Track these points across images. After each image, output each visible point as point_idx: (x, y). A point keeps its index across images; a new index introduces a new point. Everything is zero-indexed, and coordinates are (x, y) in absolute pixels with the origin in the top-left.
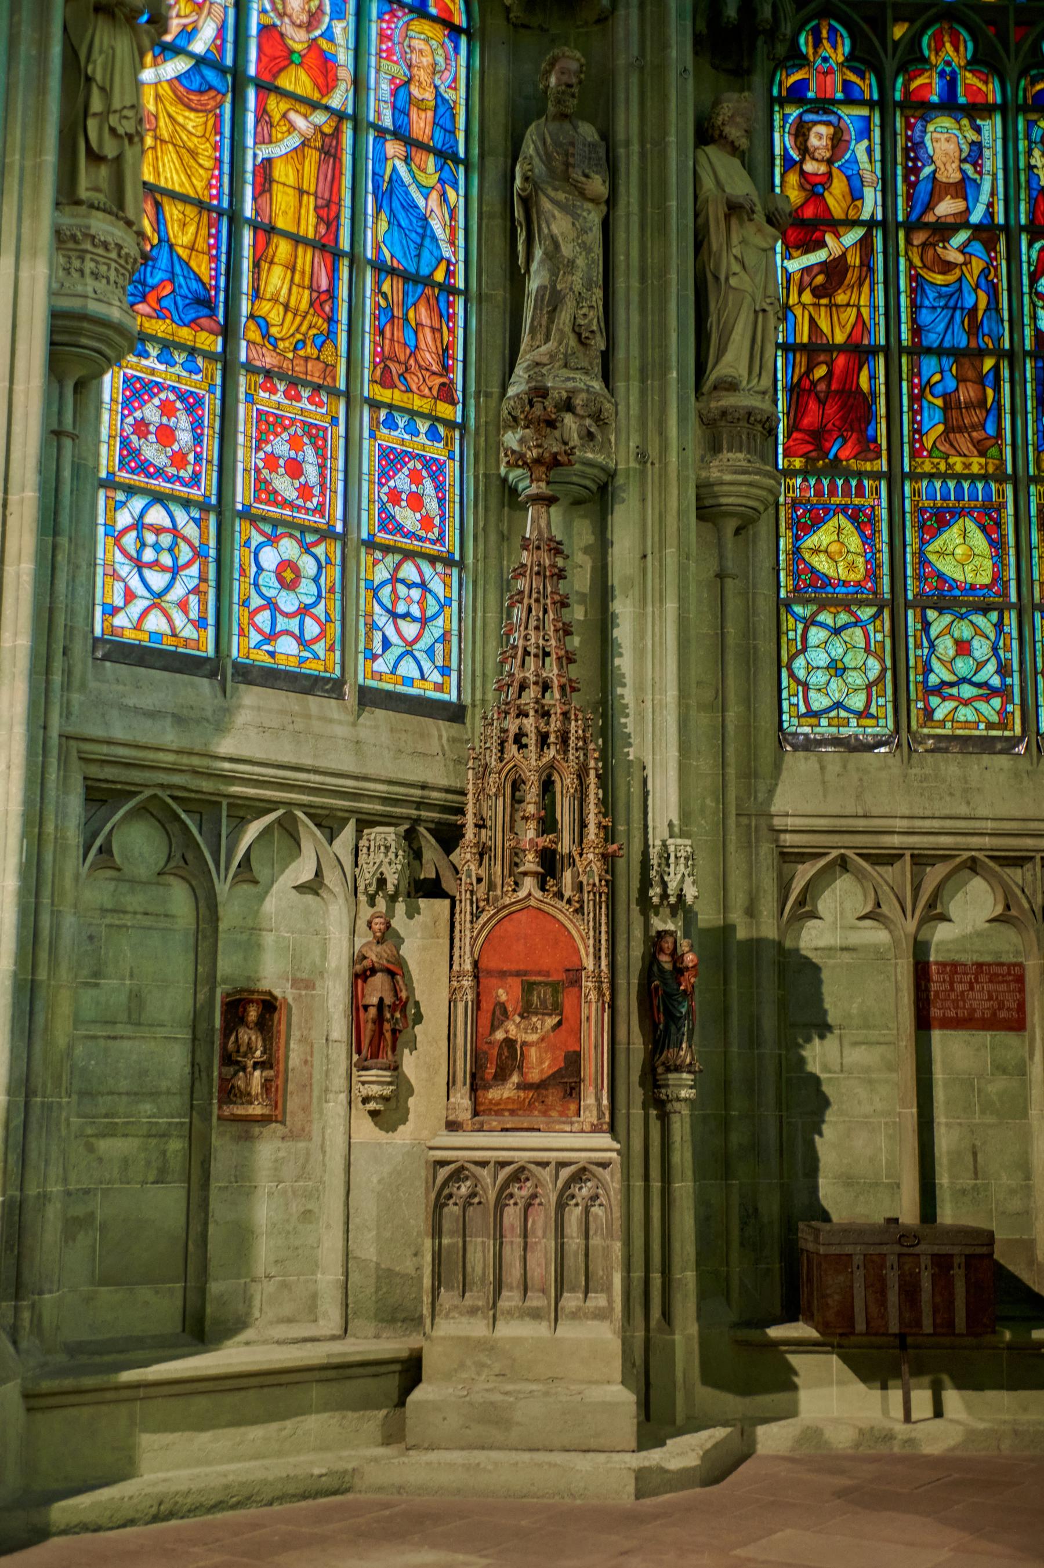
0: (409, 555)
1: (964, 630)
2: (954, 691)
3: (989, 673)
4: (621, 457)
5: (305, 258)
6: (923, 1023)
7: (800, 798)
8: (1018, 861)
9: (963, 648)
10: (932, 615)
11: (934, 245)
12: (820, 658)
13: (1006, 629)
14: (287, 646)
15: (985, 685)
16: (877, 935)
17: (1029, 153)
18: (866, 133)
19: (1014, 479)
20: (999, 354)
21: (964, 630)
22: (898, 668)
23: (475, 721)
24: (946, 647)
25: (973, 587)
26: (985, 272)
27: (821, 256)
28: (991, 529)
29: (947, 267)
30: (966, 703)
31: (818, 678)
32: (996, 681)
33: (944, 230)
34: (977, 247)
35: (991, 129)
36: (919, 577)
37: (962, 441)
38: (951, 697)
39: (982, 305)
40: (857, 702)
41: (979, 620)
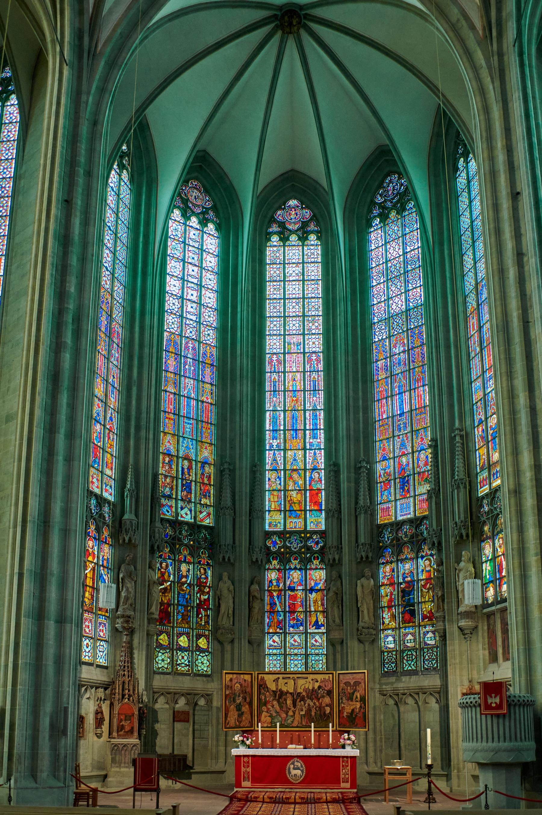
0: (102, 640)
3: (186, 662)
4: (136, 625)
5: (91, 590)
6: (174, 721)
9: (183, 657)
14: (87, 658)
16: (167, 706)
18: (171, 565)
19: (192, 629)
20: (191, 607)
22: (172, 660)
23: (110, 669)
24: (180, 657)
27: (163, 587)
28: (188, 637)
31: (160, 662)
33: (183, 584)
37: (184, 622)
40: (166, 666)
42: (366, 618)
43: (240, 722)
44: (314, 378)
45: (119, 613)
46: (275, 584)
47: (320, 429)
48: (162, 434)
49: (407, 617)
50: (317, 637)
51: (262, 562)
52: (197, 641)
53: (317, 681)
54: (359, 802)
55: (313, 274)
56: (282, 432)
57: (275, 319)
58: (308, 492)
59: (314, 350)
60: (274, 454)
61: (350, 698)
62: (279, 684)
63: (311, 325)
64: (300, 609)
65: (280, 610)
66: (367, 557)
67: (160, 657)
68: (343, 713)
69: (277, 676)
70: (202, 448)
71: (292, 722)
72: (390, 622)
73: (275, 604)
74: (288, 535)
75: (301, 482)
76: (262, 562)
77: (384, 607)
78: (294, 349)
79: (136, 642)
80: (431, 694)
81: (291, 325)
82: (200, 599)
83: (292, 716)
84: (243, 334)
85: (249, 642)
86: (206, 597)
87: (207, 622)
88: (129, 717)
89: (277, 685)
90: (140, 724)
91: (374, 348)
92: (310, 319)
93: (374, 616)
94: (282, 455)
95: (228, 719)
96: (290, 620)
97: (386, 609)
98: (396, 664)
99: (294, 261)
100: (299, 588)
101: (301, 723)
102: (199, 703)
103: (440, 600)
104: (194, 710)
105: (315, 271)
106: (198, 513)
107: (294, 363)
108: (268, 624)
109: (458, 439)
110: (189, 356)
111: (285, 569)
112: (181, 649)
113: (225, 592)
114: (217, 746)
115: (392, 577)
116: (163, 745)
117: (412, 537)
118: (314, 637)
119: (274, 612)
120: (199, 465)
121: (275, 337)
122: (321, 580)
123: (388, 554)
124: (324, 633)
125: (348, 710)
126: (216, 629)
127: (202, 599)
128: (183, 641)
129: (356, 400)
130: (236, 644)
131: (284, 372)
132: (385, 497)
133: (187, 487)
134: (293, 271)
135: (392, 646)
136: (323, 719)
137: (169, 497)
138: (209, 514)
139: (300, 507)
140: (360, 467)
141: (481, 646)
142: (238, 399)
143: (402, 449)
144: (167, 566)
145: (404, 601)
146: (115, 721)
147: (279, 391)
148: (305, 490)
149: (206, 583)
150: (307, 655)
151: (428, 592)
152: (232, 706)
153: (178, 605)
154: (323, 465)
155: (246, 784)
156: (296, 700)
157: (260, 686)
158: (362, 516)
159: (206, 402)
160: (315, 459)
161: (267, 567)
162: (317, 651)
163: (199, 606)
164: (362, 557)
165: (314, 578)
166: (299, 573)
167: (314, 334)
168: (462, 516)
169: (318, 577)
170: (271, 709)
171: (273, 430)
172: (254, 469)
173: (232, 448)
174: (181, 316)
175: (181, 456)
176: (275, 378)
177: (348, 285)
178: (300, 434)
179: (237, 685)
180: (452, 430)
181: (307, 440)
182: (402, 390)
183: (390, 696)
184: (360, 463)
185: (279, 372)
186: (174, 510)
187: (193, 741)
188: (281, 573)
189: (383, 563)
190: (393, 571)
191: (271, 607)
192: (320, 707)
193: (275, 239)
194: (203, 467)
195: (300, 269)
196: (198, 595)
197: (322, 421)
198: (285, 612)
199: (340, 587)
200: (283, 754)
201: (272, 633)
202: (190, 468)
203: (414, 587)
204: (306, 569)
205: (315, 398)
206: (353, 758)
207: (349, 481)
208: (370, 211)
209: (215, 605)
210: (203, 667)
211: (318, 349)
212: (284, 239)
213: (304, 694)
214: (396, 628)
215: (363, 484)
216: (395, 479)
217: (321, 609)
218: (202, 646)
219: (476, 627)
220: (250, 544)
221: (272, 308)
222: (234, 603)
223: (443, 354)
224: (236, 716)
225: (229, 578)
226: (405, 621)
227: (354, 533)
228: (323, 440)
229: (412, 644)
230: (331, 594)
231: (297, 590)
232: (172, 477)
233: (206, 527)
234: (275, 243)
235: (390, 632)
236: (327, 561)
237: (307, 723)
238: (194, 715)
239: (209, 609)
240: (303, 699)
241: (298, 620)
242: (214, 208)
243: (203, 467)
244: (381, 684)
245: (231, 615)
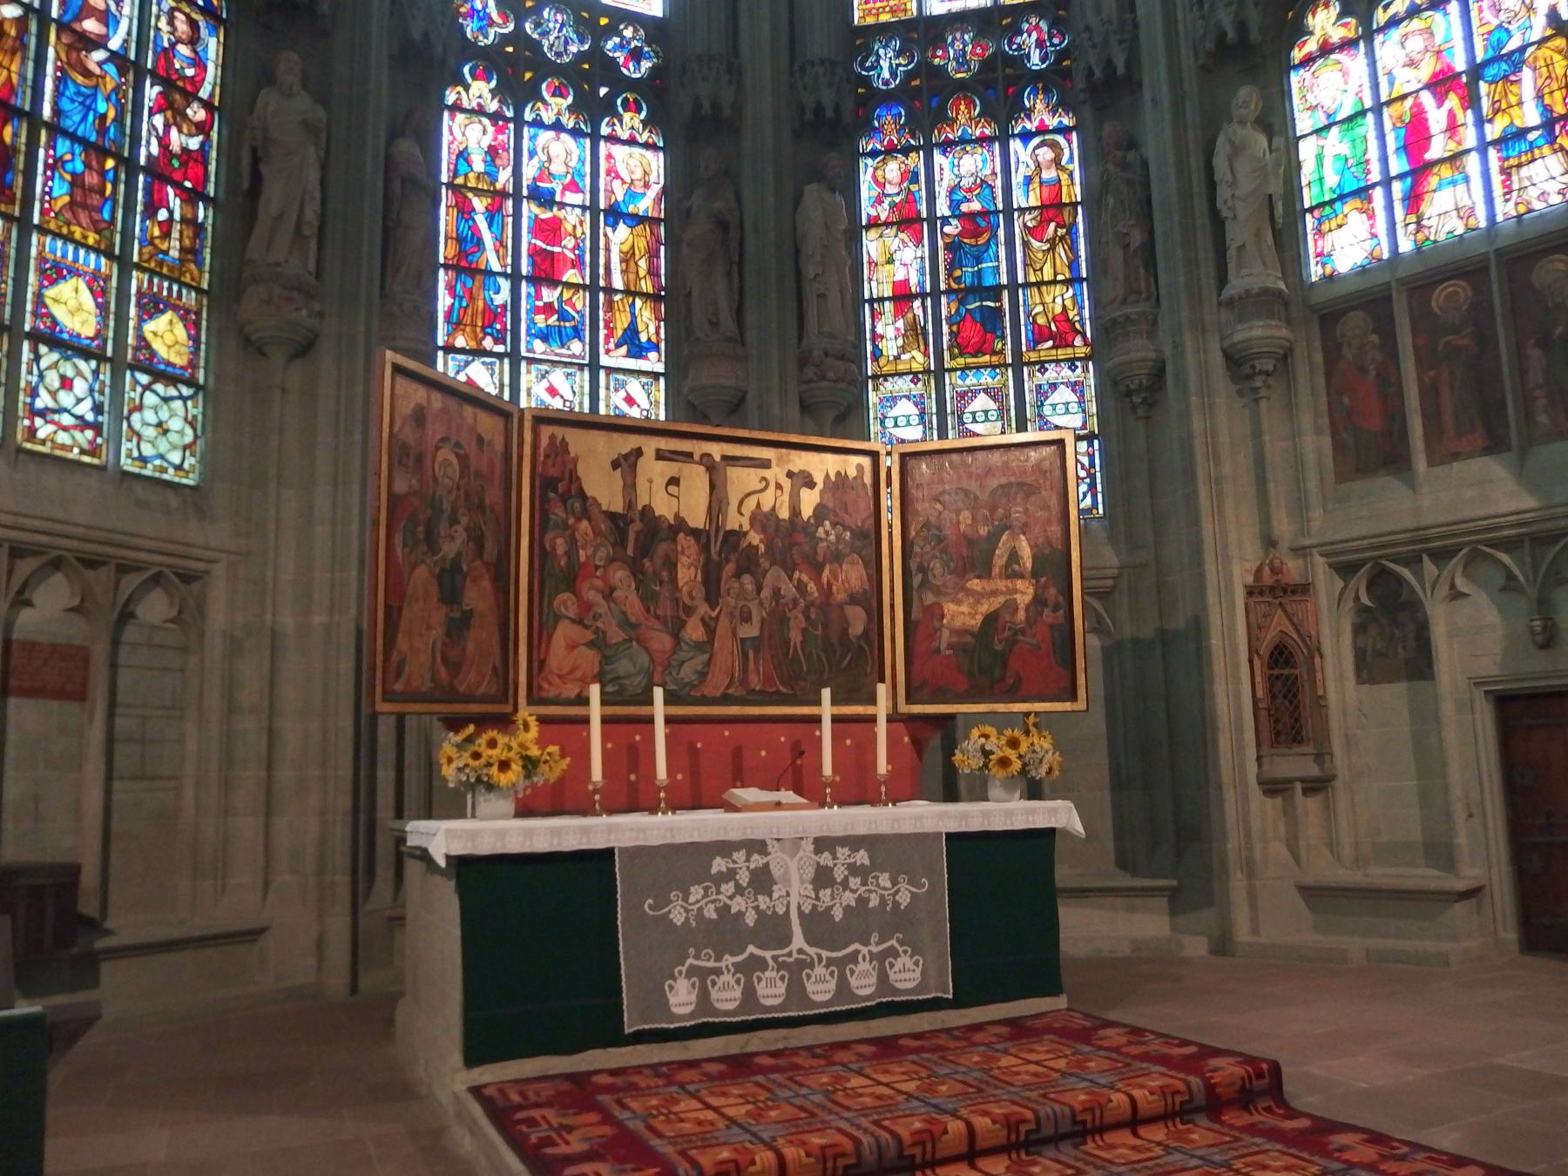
2: (56, 417)
3: (85, 409)
8: (92, 563)
9: (66, 383)
10: (43, 349)
11: (79, 51)
13: (101, 377)
15: (80, 418)
17: (158, 18)
24: (53, 379)
25: (79, 336)
26: (117, 89)
28: (99, 294)
29: (87, 73)
30: (65, 429)
32: (90, 417)
34: (111, 69)
36: (35, 314)
38: (52, 422)
39: (112, 114)
41: (82, 364)
43: (455, 668)
46: (479, 166)
49: (972, 334)
52: (141, 321)
53: (811, 484)
61: (974, 559)
64: (571, 276)
65: (495, 266)
68: (934, 633)
69: (632, 441)
71: (703, 675)
72: (903, 350)
73: (479, 243)
77: (881, 300)
82: (164, 142)
83: (699, 646)
86: (194, 143)
95: (402, 643)
97: (888, 306)
100: (571, 198)
101: (744, 681)
102: (140, 610)
104: (116, 643)
108: (448, 315)
115: (911, 199)
118: (621, 386)
122: (647, 186)
123: (890, 124)
125: (962, 614)
127: (175, 146)
149: (197, 82)
151: (1052, 249)
152: (421, 573)
156: (720, 567)
157: (545, 485)
163: (159, 173)
164: (819, 109)
169: (638, 174)
170: (602, 606)
179: (445, 454)
187: (108, 792)
188: (500, 131)
190: (915, 178)
191: (462, 254)
196: (159, 120)
198: (515, 278)
201: (462, 351)
203: (995, 236)
204: (595, 138)
210: (163, 445)
213: (755, 538)
214: (927, 371)
217: (646, 286)
218: (162, 352)
222: (323, 183)
224: (437, 633)
226: (961, 346)
231: (562, 205)
235: (903, 384)
237: (768, 679)
238: (114, 666)
241: (563, 316)
245: (310, 231)
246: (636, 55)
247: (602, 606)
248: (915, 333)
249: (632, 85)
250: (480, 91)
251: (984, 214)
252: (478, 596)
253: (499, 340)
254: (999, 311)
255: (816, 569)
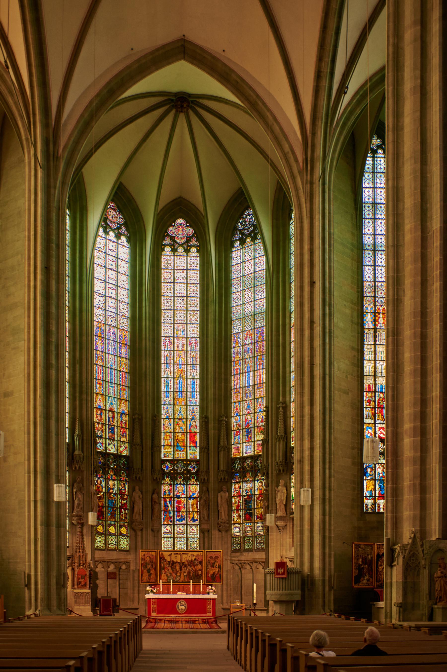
1: (112, 538)
3: (114, 543)
6: (108, 579)
7: (98, 555)
8: (116, 562)
9: (112, 540)
12: (99, 540)
16: (103, 570)
21: (112, 538)
22: (106, 542)
24: (110, 540)
31: (98, 543)
35: (116, 482)
42: (223, 517)
43: (150, 579)
44: (193, 356)
45: (74, 513)
46: (168, 493)
47: (196, 392)
48: (95, 395)
49: (248, 516)
50: (194, 527)
51: (160, 479)
53: (194, 556)
54: (216, 623)
55: (194, 278)
56: (172, 393)
57: (168, 311)
58: (188, 434)
59: (193, 335)
60: (167, 408)
61: (213, 566)
62: (172, 557)
63: (191, 317)
64: (183, 510)
65: (170, 510)
66: (224, 479)
67: (98, 539)
70: (120, 403)
72: (237, 519)
73: (168, 506)
74: (176, 462)
75: (184, 427)
76: (160, 479)
78: (180, 334)
79: (85, 531)
80: (260, 563)
81: (178, 317)
82: (121, 503)
83: (179, 576)
84: (146, 324)
85: (152, 530)
86: (125, 502)
87: (126, 518)
88: (84, 577)
89: (171, 558)
90: (90, 581)
91: (233, 338)
92: (191, 312)
93: (228, 515)
94: (172, 409)
95: (143, 577)
96: (177, 516)
98: (240, 545)
99: (181, 268)
100: (183, 496)
102: (122, 567)
103: (267, 508)
104: (119, 572)
105: (195, 277)
106: (119, 447)
107: (180, 344)
108: (163, 519)
109: (281, 409)
110: (111, 339)
111: (174, 484)
112: (111, 534)
113: (137, 499)
114: (134, 593)
115: (240, 492)
116: (101, 592)
117: (252, 467)
118: (191, 527)
119: (167, 511)
120: (119, 415)
121: (167, 325)
124: (197, 525)
125: (211, 572)
126: (131, 522)
127: (123, 503)
128: (112, 530)
129: (220, 374)
130: (144, 532)
131: (174, 351)
132: (236, 441)
133: (112, 430)
134: (180, 275)
135: (238, 534)
136: (197, 578)
137: (101, 437)
138: (126, 448)
139: (184, 443)
140: (222, 420)
141: (288, 536)
142: (144, 370)
143: (248, 409)
144: (101, 482)
145: (246, 507)
146: (76, 579)
147: (170, 364)
148: (187, 433)
149: (125, 492)
150: (187, 538)
151: (260, 502)
153: (108, 507)
154: (198, 416)
155: (154, 614)
157: (161, 558)
158: (222, 452)
159: (122, 371)
160: (193, 412)
161: (163, 482)
162: (193, 536)
163: (121, 507)
165: (192, 490)
166: (183, 487)
167: (194, 324)
168: (281, 458)
170: (167, 572)
171: (166, 391)
172: (155, 418)
173: (140, 404)
174: (105, 310)
175: (107, 409)
176: (167, 355)
177: (217, 291)
178: (184, 395)
179: (148, 558)
180: (278, 403)
181: (188, 399)
182: (249, 370)
183: (237, 564)
184: (222, 417)
185: (170, 350)
186: (104, 445)
187: (119, 590)
188: (171, 486)
189: (234, 483)
190: (240, 488)
191: (165, 508)
192: (195, 571)
193: (168, 249)
194: (121, 416)
195: (184, 275)
196: (120, 500)
197: (198, 386)
198: (174, 511)
199: (208, 496)
200: (174, 597)
202: (113, 417)
204: (187, 485)
205: (193, 370)
206: (214, 600)
207: (214, 429)
208: (233, 235)
209: (130, 506)
210: (124, 545)
211: (196, 335)
212: (174, 250)
213: (186, 563)
215: (223, 432)
216: (243, 429)
218: (123, 532)
219: (286, 525)
220: (152, 468)
221: (166, 302)
222: (142, 505)
223: (274, 351)
224: (147, 576)
225: (139, 490)
226: (246, 519)
227: (217, 463)
228: (198, 400)
229: (250, 533)
230: (202, 501)
232: (103, 424)
233: (124, 457)
234: (168, 253)
235: (237, 525)
236: (200, 480)
238: (119, 575)
239: (127, 509)
240: (185, 566)
241: (182, 517)
242: (125, 224)
243: (121, 416)
244: (231, 557)
245: (141, 514)
246: (194, 468)
247: (167, 572)
248: (239, 516)
249: (193, 473)
250: (167, 480)
251: (251, 495)
252: (152, 572)
253: (171, 522)
254: (252, 513)
255: (194, 566)
